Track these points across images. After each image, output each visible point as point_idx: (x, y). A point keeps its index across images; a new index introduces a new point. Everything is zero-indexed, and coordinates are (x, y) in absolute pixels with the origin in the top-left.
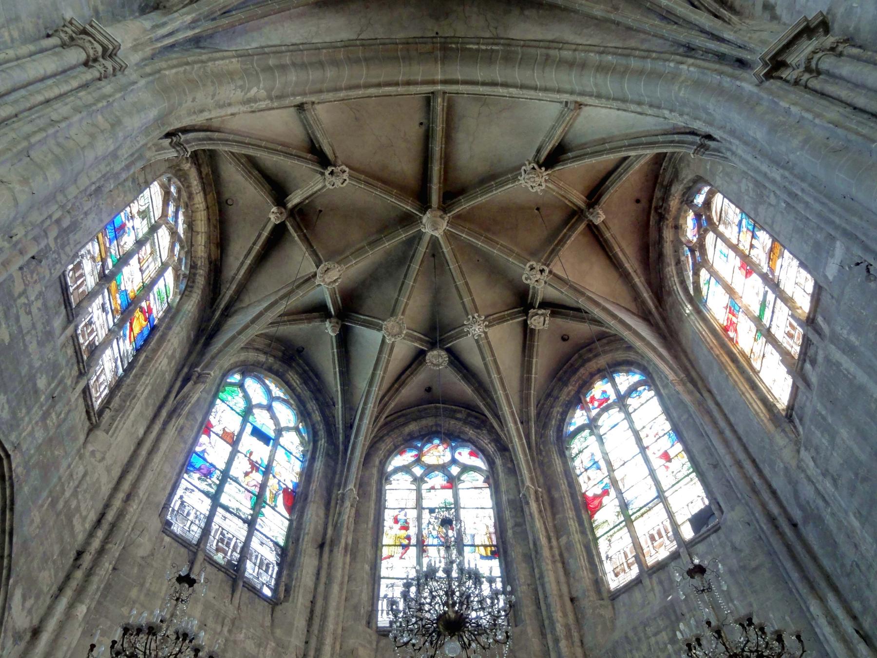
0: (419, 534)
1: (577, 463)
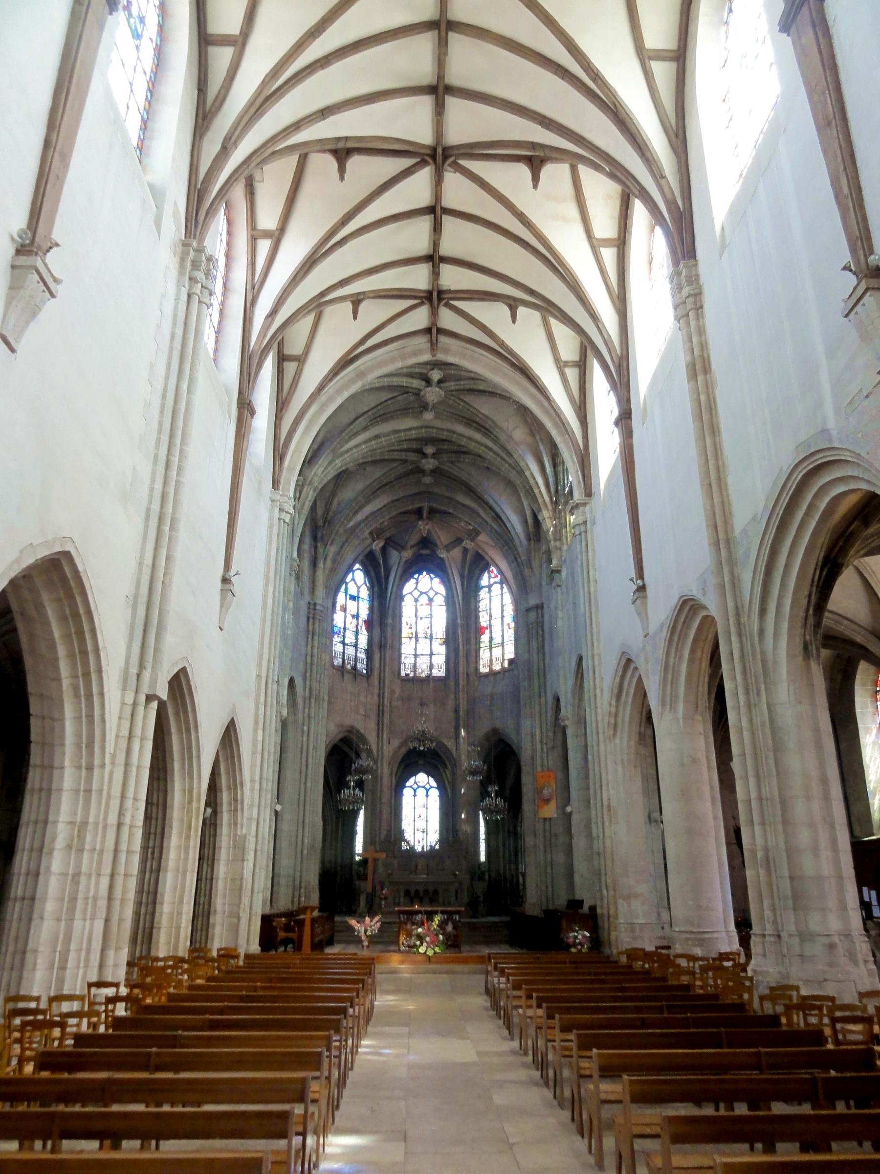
0: (416, 632)
1: (480, 604)
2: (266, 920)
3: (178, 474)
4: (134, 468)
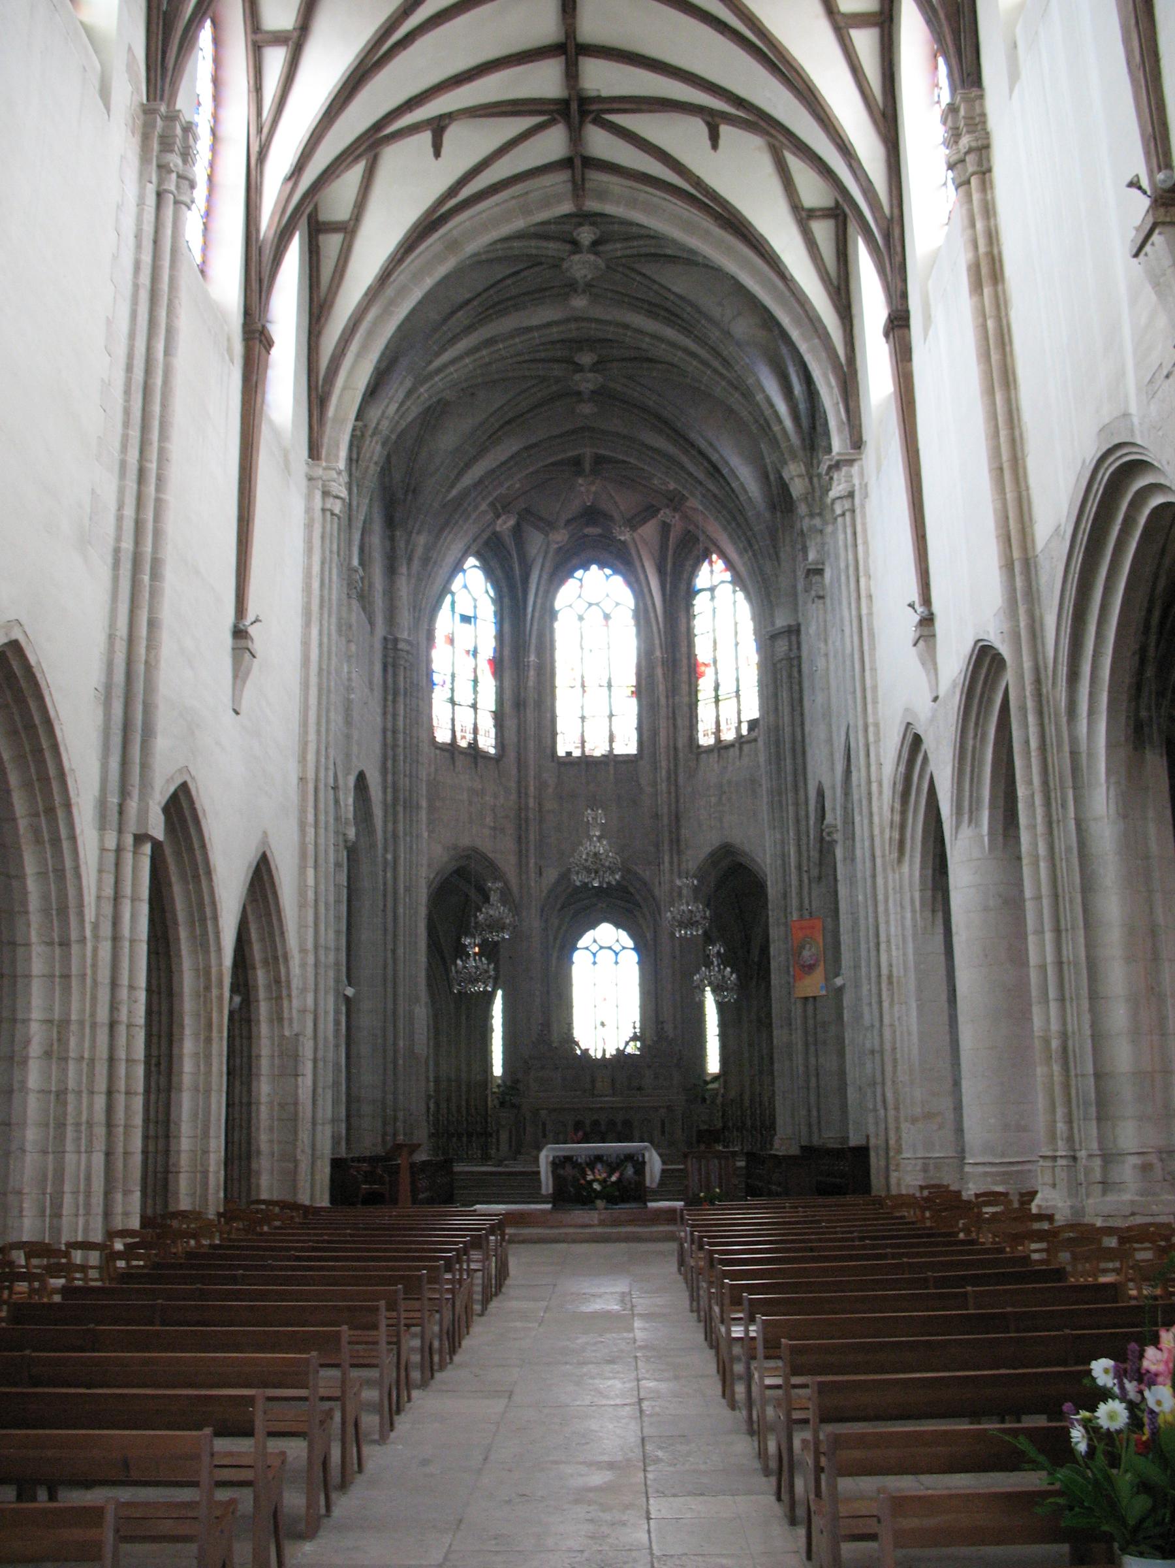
2: (337, 1164)
3: (159, 489)
4: (93, 491)
